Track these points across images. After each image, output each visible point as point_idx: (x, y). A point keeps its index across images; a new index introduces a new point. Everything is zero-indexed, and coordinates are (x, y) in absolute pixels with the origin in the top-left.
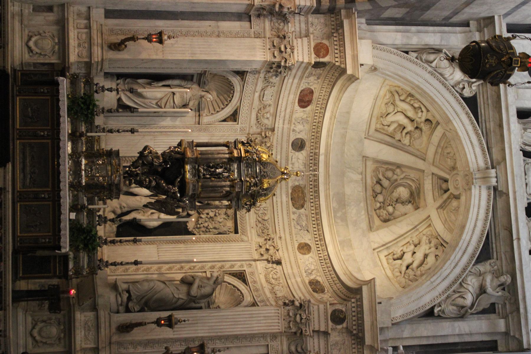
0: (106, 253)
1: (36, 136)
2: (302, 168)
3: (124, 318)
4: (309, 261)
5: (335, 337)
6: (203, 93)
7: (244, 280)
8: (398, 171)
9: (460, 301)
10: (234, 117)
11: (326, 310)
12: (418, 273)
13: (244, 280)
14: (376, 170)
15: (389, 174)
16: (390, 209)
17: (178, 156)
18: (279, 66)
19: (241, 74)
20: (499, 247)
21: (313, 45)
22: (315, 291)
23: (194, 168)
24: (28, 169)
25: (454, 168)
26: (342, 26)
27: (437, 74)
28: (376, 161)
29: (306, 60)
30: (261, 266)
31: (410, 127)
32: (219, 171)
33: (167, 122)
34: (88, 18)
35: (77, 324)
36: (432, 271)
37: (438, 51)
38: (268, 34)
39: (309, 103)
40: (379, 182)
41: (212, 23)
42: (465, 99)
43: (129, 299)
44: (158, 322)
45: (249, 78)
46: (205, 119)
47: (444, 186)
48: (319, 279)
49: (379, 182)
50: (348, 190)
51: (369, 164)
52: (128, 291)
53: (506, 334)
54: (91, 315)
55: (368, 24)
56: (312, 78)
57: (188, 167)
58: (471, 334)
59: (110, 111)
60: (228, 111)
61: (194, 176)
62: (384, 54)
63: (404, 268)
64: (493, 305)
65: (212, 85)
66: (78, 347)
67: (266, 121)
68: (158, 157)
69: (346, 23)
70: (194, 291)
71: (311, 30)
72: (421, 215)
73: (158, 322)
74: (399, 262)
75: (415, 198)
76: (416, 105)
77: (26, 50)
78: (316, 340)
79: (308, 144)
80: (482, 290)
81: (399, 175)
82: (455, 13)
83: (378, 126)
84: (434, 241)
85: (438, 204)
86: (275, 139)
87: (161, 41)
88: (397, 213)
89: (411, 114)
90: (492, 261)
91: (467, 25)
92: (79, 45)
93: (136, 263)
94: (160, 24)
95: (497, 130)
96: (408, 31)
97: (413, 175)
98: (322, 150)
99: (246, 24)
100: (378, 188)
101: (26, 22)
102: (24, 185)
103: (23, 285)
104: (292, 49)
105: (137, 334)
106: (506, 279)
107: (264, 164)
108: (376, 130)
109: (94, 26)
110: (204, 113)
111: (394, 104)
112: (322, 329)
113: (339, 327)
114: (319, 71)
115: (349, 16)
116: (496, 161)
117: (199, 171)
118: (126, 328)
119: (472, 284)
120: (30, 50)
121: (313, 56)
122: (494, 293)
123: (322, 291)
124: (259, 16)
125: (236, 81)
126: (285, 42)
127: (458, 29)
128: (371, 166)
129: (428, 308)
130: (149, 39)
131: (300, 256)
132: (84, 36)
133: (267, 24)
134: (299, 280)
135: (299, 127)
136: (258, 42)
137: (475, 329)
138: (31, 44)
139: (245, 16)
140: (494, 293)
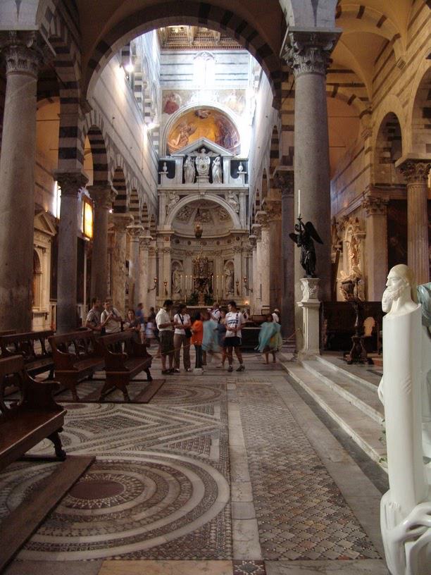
3: (235, 293)
5: (243, 240)
10: (182, 261)
19: (172, 260)
27: (173, 207)
30: (222, 256)
37: (167, 206)
46: (182, 269)
57: (201, 277)
60: (180, 263)
69: (161, 233)
70: (229, 274)
80: (233, 199)
91: (159, 196)
105: (240, 290)
115: (158, 231)
116: (198, 191)
118: (238, 293)
119: (231, 201)
122: (233, 196)
137: (242, 201)
139: (157, 260)
140: (233, 196)
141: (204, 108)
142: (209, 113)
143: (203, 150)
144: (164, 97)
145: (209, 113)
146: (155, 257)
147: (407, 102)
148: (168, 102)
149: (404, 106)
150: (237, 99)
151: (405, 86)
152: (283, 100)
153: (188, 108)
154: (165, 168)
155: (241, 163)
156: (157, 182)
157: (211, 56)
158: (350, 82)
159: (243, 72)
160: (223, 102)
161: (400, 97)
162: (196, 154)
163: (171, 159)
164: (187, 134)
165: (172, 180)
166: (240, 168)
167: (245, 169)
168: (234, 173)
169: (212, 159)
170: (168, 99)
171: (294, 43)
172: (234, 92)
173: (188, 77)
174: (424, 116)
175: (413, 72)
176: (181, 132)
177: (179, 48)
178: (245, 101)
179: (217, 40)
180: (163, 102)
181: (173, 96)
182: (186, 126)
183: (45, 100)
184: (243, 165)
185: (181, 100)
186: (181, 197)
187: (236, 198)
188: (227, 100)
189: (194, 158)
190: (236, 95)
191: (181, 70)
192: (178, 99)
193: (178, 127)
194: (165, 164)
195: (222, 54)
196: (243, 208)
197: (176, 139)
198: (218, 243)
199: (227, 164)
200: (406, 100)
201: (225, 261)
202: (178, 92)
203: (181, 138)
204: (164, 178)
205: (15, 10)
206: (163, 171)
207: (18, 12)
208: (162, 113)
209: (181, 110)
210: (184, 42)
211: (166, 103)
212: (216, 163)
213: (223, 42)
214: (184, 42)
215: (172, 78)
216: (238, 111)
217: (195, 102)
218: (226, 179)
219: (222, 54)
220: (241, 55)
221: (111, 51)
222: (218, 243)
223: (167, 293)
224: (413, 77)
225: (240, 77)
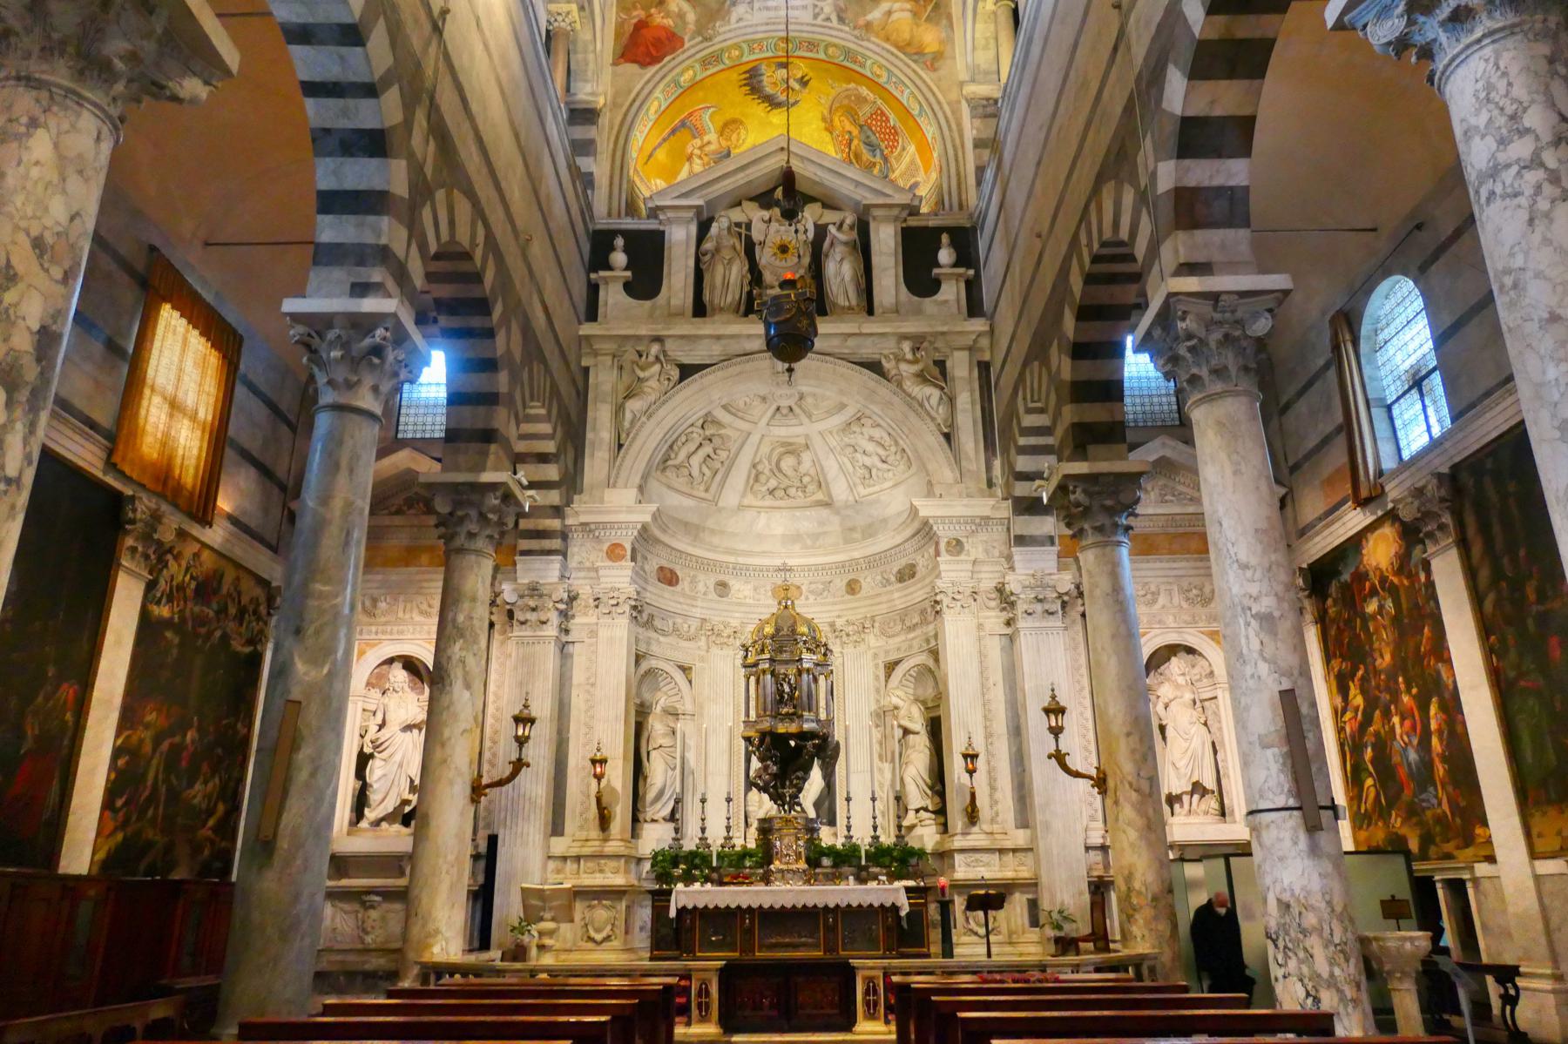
0: (862, 837)
1: (750, 930)
2: (750, 586)
4: (868, 582)
6: (659, 708)
7: (897, 663)
8: (760, 467)
9: (934, 401)
10: (685, 669)
11: (949, 562)
12: (893, 449)
13: (897, 663)
14: (755, 494)
15: (763, 478)
16: (806, 479)
17: (768, 740)
18: (635, 608)
19: (638, 659)
20: (868, 350)
21: (610, 563)
22: (913, 576)
23: (782, 720)
24: (796, 940)
25: (764, 399)
26: (587, 524)
28: (744, 495)
29: (629, 572)
31: (708, 449)
32: (787, 689)
33: (691, 756)
34: (564, 858)
35: (971, 876)
38: (593, 620)
39: (672, 572)
40: (771, 492)
41: (574, 693)
42: (682, 379)
43: (926, 809)
44: (971, 772)
45: (643, 648)
47: (785, 411)
48: (895, 570)
49: (771, 492)
50: (778, 530)
51: (746, 502)
52: (917, 811)
53: (970, 349)
54: (959, 859)
55: (581, 492)
56: (647, 567)
57: (781, 729)
58: (972, 391)
59: (677, 830)
60: (679, 676)
61: (792, 721)
62: (623, 474)
63: (885, 466)
64: (936, 363)
65: (647, 696)
66: (999, 875)
67: (693, 629)
68: (766, 768)
69: (583, 519)
71: (588, 564)
72: (817, 442)
73: (971, 772)
74: (874, 472)
75: (791, 449)
76: (683, 439)
77: (606, 945)
78: (983, 575)
79: (721, 577)
81: (765, 467)
82: (574, 381)
83: (702, 488)
84: (855, 428)
85: (805, 420)
86: (716, 619)
87: (603, 762)
88: (812, 472)
89: (692, 447)
90: (884, 361)
92: (601, 871)
93: (873, 799)
94: (577, 760)
95: (723, 342)
96: (593, 444)
97: (765, 449)
98: (732, 559)
99: (576, 650)
100: (780, 493)
101: (568, 946)
102: (816, 946)
103: (935, 948)
104: (613, 589)
106: (906, 346)
107: (778, 630)
108: (707, 490)
109: (574, 852)
110: (680, 708)
111: (677, 467)
112: (970, 567)
113: (966, 546)
114: (639, 558)
117: (787, 714)
120: (607, 939)
121: (623, 563)
123: (913, 566)
124: (567, 631)
125: (644, 666)
126: (604, 599)
127: (591, 380)
128: (749, 500)
129: (942, 439)
130: (599, 777)
131: (863, 593)
132: (590, 864)
133: (577, 620)
134: (896, 595)
135: (701, 587)
136: (603, 633)
138: (599, 937)
146: (551, 631)
148: (641, 25)
150: (915, 14)
154: (619, 258)
155: (945, 238)
156: (582, 308)
160: (861, 22)
162: (756, 214)
165: (648, 304)
166: (945, 256)
167: (966, 256)
168: (921, 280)
170: (639, 13)
176: (690, 158)
178: (949, 17)
182: (712, 136)
184: (954, 244)
185: (691, 17)
186: (687, 371)
187: (936, 371)
188: (875, 15)
192: (681, 16)
194: (619, 242)
198: (852, 587)
199: (885, 239)
201: (891, 667)
204: (613, 296)
206: (610, 268)
208: (615, 64)
211: (629, 28)
212: (840, 236)
222: (852, 587)
223: (604, 821)
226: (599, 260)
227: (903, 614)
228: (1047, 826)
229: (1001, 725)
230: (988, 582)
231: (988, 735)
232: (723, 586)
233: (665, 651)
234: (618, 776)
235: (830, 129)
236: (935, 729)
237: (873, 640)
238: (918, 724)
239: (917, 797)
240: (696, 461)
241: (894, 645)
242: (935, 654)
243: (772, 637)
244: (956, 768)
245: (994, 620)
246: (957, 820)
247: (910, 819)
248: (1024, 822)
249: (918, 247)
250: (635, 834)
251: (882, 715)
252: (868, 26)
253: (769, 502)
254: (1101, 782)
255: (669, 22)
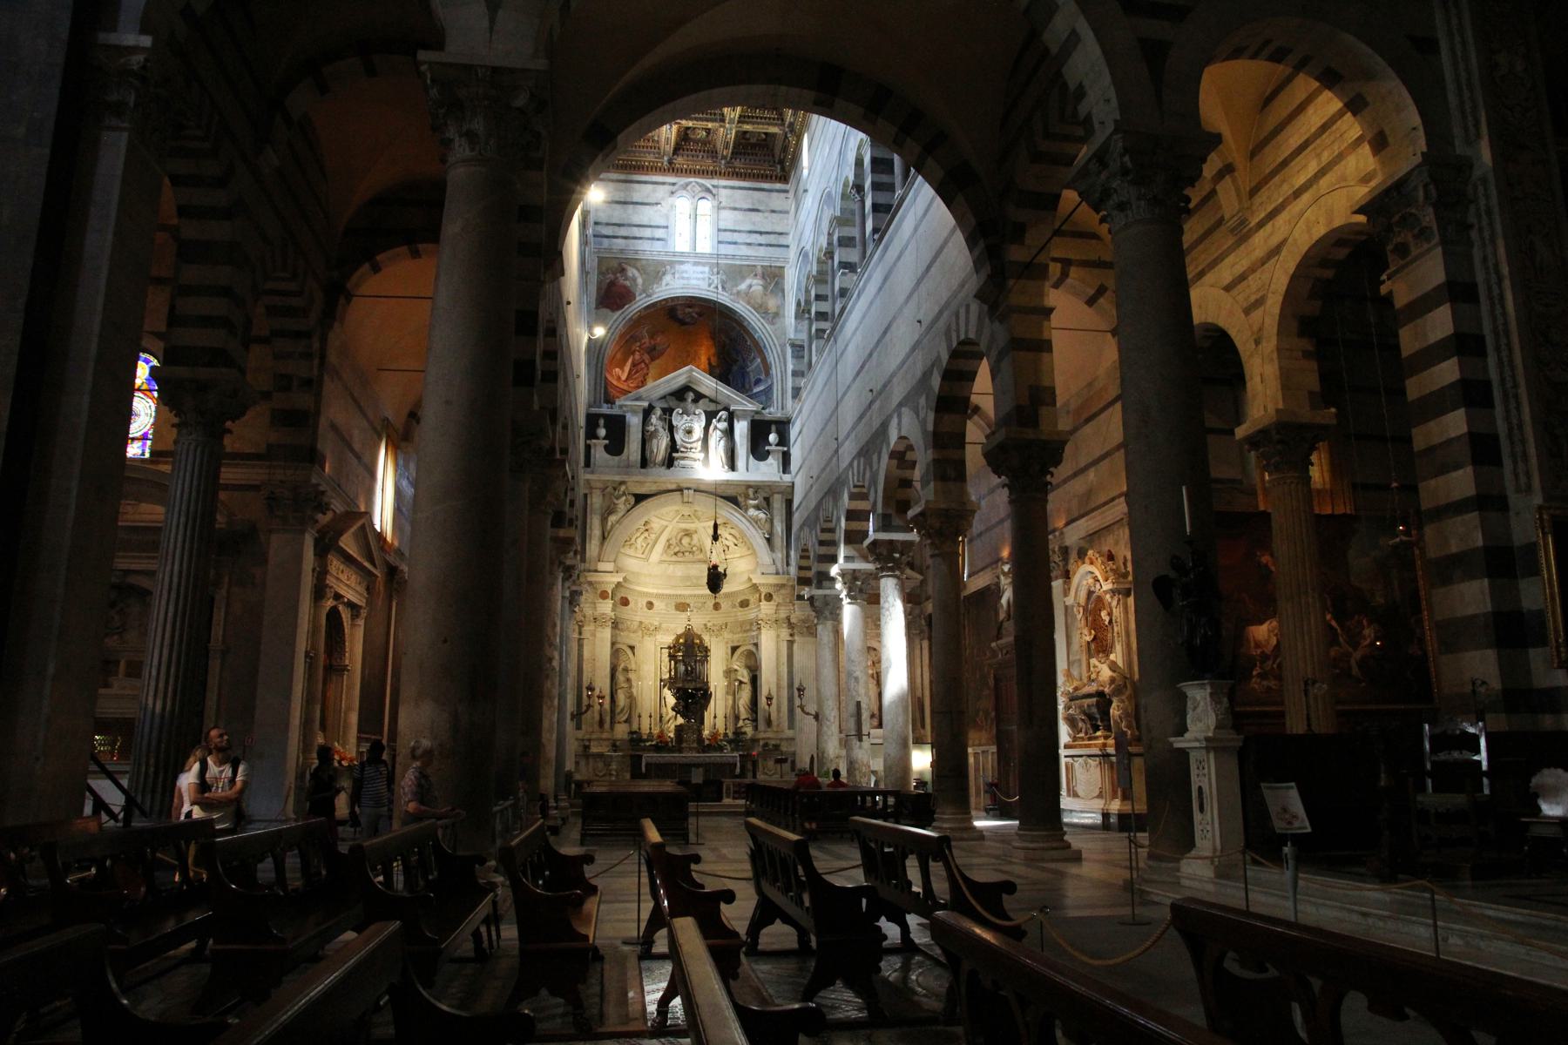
20: (730, 492)
36: (741, 532)
46: (633, 666)
60: (629, 652)
75: (688, 534)
80: (757, 508)
81: (673, 542)
86: (646, 622)
106: (751, 491)
119: (752, 512)
128: (665, 558)
141: (693, 302)
142: (700, 315)
143: (691, 396)
144: (600, 273)
145: (700, 315)
147: (1259, 302)
148: (612, 284)
149: (1247, 311)
150: (765, 288)
151: (1253, 269)
152: (1011, 282)
153: (655, 298)
154: (602, 432)
155: (773, 428)
157: (708, 190)
158: (1093, 257)
159: (779, 229)
161: (1235, 292)
163: (615, 411)
164: (646, 357)
166: (773, 437)
167: (783, 440)
168: (758, 449)
169: (710, 416)
170: (611, 276)
171: (1122, 156)
172: (759, 270)
173: (659, 233)
174: (1301, 334)
175: (1274, 241)
176: (633, 353)
177: (639, 168)
178: (783, 291)
179: (724, 157)
180: (599, 283)
181: (623, 270)
182: (646, 340)
183: (404, 249)
185: (640, 281)
188: (743, 286)
189: (668, 412)
190: (763, 277)
191: (646, 215)
192: (634, 280)
193: (628, 340)
194: (602, 422)
195: (733, 188)
196: (779, 528)
197: (622, 369)
199: (741, 428)
200: (1253, 298)
201: (734, 649)
202: (634, 262)
203: (634, 365)
204: (599, 454)
205: (485, 23)
206: (597, 438)
207: (491, 29)
208: (597, 308)
209: (641, 302)
210: (650, 158)
211: (604, 286)
213: (737, 163)
214: (650, 158)
215: (623, 232)
216: (766, 313)
217: (676, 285)
218: (741, 462)
219: (733, 188)
220: (775, 195)
221: (615, 148)
223: (601, 723)
224: (1276, 251)
225: (772, 239)
226: (591, 434)
227: (742, 624)
228: (801, 729)
229: (785, 683)
230: (783, 614)
231: (779, 687)
232: (650, 605)
233: (626, 638)
234: (607, 706)
235: (713, 339)
236: (755, 680)
237: (726, 635)
238: (746, 679)
239: (744, 714)
240: (640, 540)
241: (736, 638)
242: (756, 645)
243: (685, 644)
244: (763, 701)
245: (785, 633)
246: (762, 726)
247: (741, 723)
248: (791, 726)
249: (759, 431)
250: (612, 728)
251: (729, 673)
252: (738, 293)
253: (674, 558)
254: (817, 717)
255: (628, 283)
